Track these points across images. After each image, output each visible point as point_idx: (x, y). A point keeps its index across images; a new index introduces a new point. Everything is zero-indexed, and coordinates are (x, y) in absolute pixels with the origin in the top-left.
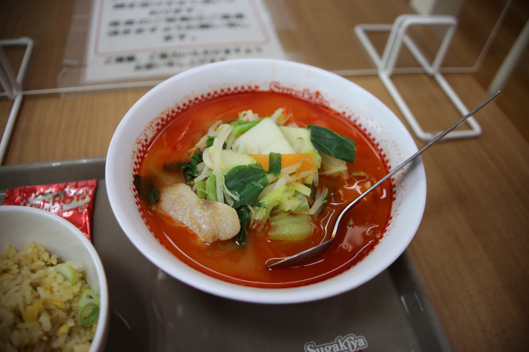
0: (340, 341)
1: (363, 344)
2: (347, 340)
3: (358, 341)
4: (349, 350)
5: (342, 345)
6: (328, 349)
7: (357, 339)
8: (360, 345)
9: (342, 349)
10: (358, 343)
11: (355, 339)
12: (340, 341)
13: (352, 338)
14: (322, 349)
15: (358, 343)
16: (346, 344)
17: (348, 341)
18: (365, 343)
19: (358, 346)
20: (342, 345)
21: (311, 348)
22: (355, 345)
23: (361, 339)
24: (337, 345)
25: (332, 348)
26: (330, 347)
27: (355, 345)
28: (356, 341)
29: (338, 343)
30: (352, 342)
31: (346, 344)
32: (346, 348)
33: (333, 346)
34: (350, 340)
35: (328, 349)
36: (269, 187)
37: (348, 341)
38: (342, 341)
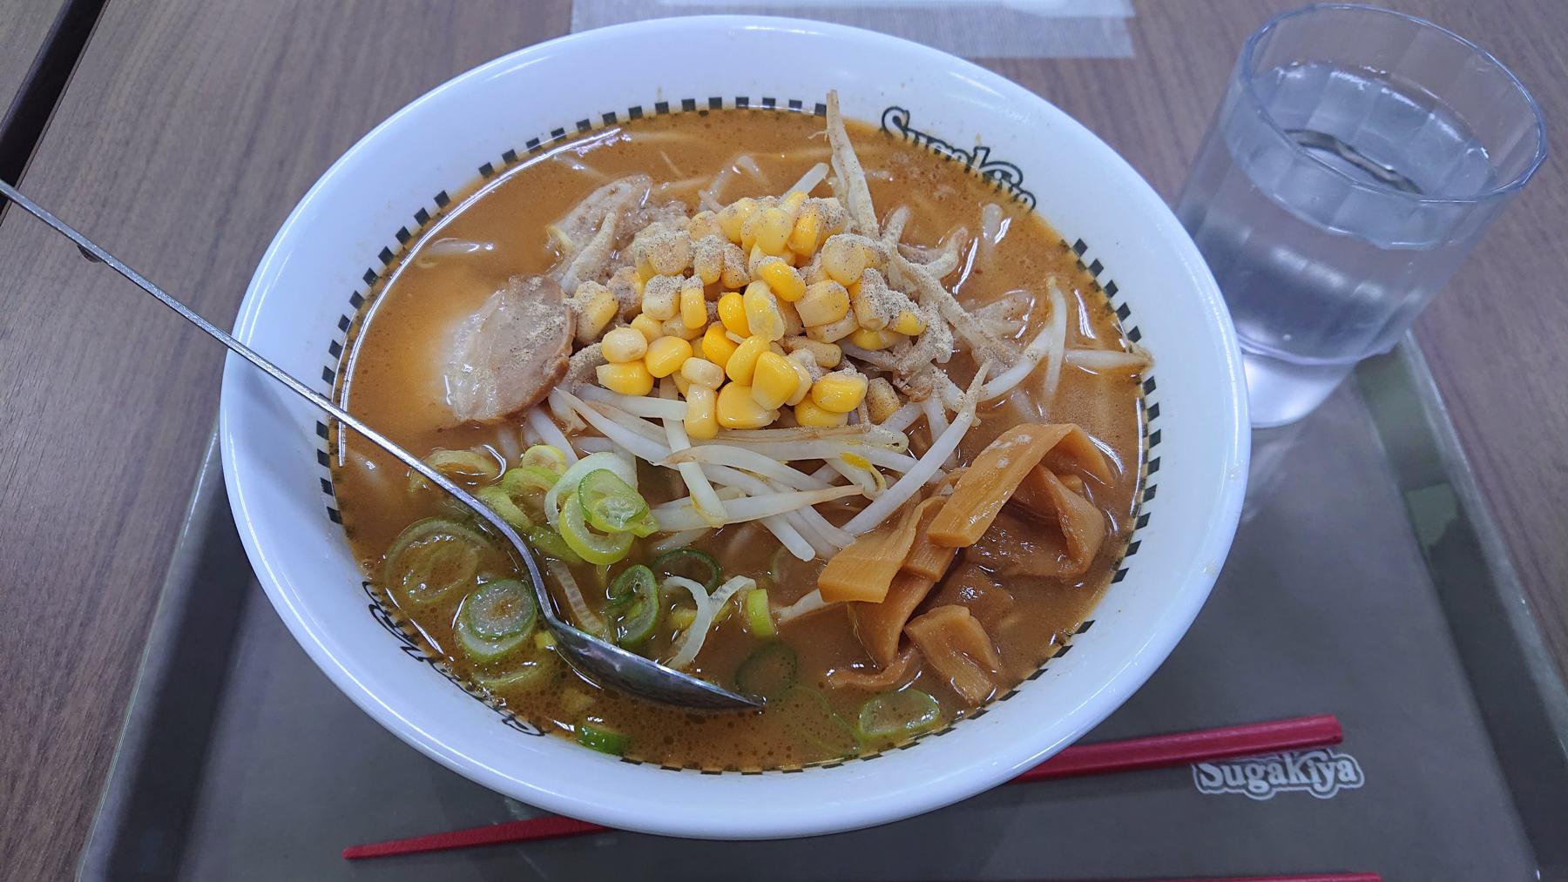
0: (1288, 760)
3: (1339, 765)
4: (1311, 785)
7: (1336, 760)
8: (1342, 777)
9: (1293, 780)
10: (1337, 770)
11: (1331, 759)
13: (1323, 756)
15: (1337, 770)
17: (1310, 763)
19: (1337, 780)
27: (1329, 775)
28: (1331, 764)
30: (1322, 766)
32: (1304, 779)
34: (1317, 760)
37: (1310, 763)
38: (1294, 762)
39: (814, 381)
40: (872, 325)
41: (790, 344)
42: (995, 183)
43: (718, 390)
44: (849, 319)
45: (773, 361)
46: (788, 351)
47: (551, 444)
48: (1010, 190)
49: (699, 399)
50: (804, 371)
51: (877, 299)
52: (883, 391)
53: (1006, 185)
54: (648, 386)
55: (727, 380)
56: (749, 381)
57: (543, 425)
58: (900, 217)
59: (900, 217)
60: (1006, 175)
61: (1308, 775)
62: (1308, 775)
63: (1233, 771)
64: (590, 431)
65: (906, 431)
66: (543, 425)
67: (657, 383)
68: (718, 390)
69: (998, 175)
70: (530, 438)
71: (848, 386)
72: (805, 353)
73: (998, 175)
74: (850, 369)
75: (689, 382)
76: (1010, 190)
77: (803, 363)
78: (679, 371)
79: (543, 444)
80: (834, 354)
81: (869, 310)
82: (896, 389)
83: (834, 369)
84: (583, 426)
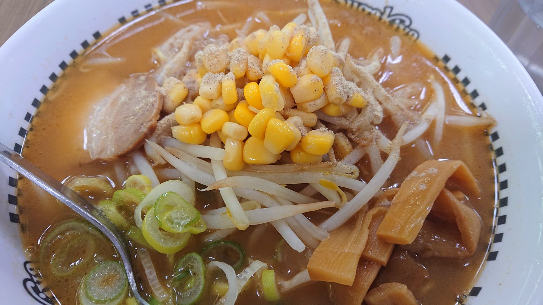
39: (302, 135)
40: (337, 101)
41: (287, 113)
42: (395, 26)
43: (244, 141)
44: (323, 98)
45: (277, 123)
46: (286, 118)
47: (144, 173)
48: (404, 29)
49: (232, 146)
50: (296, 130)
51: (340, 86)
52: (344, 142)
53: (402, 27)
54: (203, 139)
55: (249, 136)
56: (263, 136)
57: (141, 163)
58: (346, 43)
59: (346, 43)
60: (402, 22)
64: (168, 165)
65: (356, 164)
66: (141, 163)
67: (209, 136)
68: (244, 141)
69: (397, 22)
70: (133, 169)
71: (323, 138)
72: (296, 119)
73: (397, 22)
74: (323, 128)
75: (227, 137)
76: (404, 29)
77: (296, 125)
78: (221, 130)
79: (139, 173)
80: (313, 119)
81: (334, 93)
82: (350, 140)
83: (313, 128)
84: (163, 162)
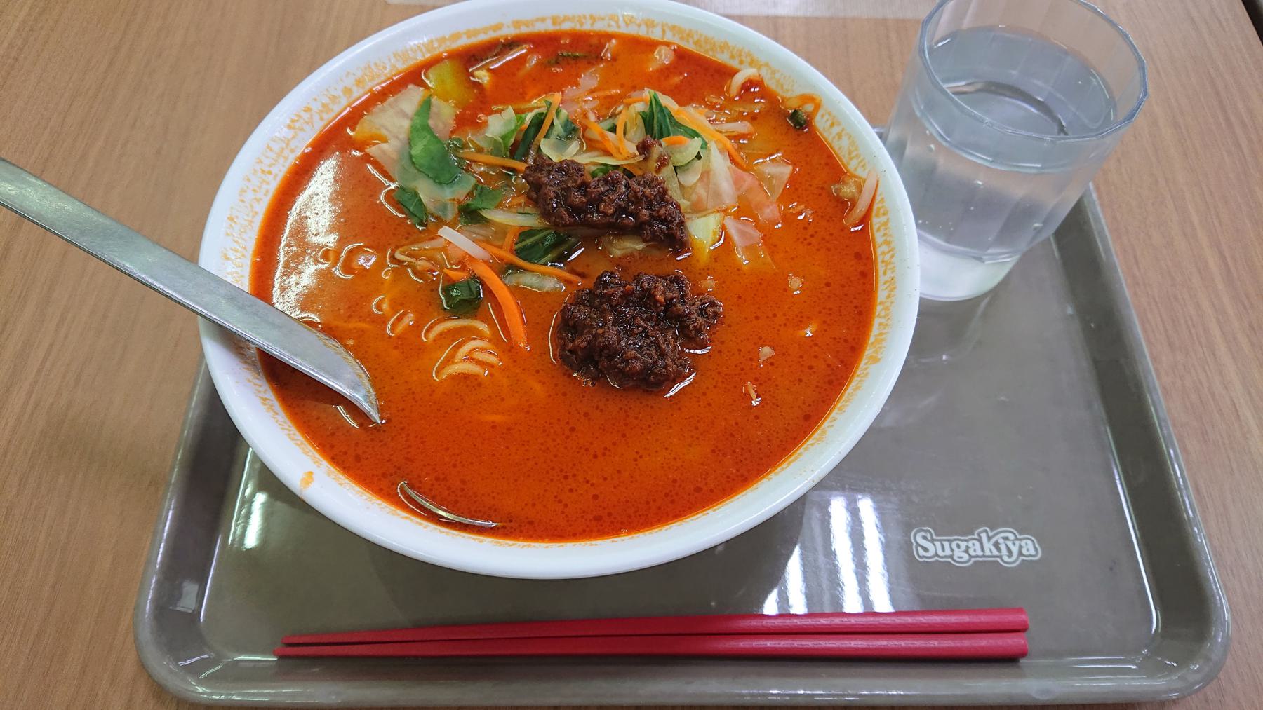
0: (984, 536)
1: (1033, 552)
2: (999, 538)
3: (1023, 544)
4: (1001, 557)
5: (988, 546)
6: (958, 546)
8: (1024, 552)
9: (988, 553)
10: (1021, 547)
11: (1017, 539)
12: (984, 536)
13: (1011, 536)
14: (946, 544)
16: (997, 545)
17: (1001, 541)
18: (1036, 549)
19: (1020, 554)
20: (988, 546)
21: (925, 538)
22: (1015, 550)
23: (1029, 542)
24: (977, 543)
25: (968, 547)
26: (963, 545)
27: (1015, 550)
28: (1017, 543)
29: (980, 540)
30: (1010, 544)
31: (997, 545)
32: (995, 552)
33: (970, 544)
34: (1006, 539)
35: (958, 546)
36: (876, 222)
37: (1001, 541)
38: (989, 538)
61: (998, 549)
62: (998, 549)
63: (854, 512)
